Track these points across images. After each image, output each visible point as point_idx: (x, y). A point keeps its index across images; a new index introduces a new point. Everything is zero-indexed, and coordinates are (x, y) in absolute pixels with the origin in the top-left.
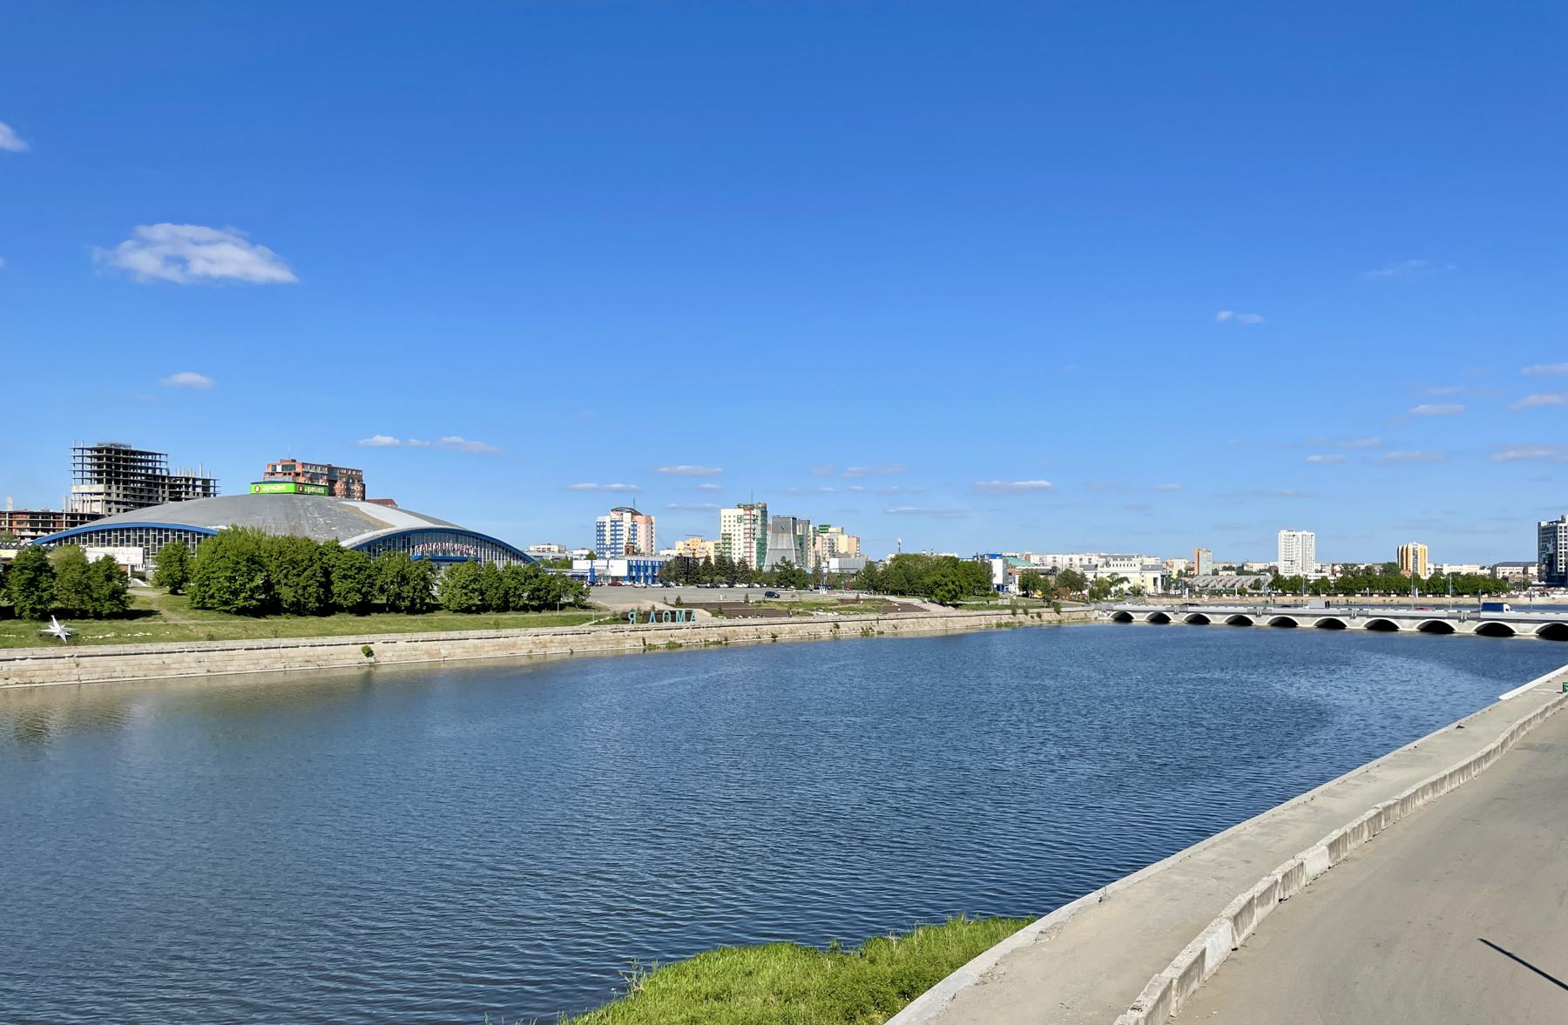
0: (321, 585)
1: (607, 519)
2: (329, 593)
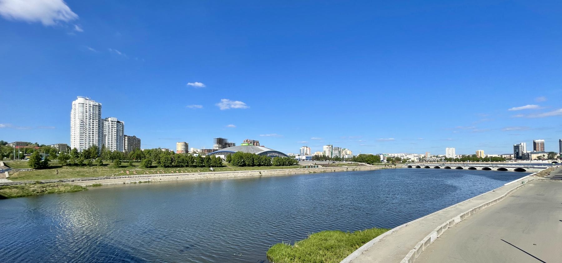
0: (252, 161)
1: (302, 148)
2: (254, 163)
